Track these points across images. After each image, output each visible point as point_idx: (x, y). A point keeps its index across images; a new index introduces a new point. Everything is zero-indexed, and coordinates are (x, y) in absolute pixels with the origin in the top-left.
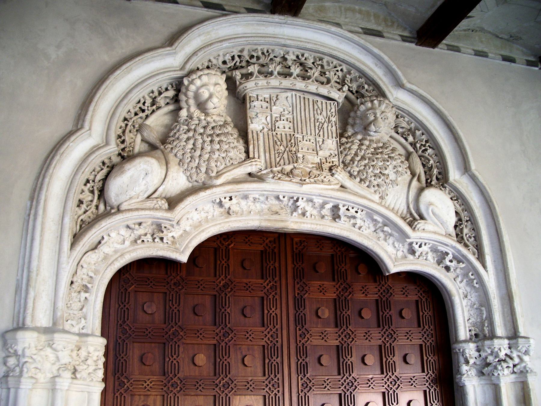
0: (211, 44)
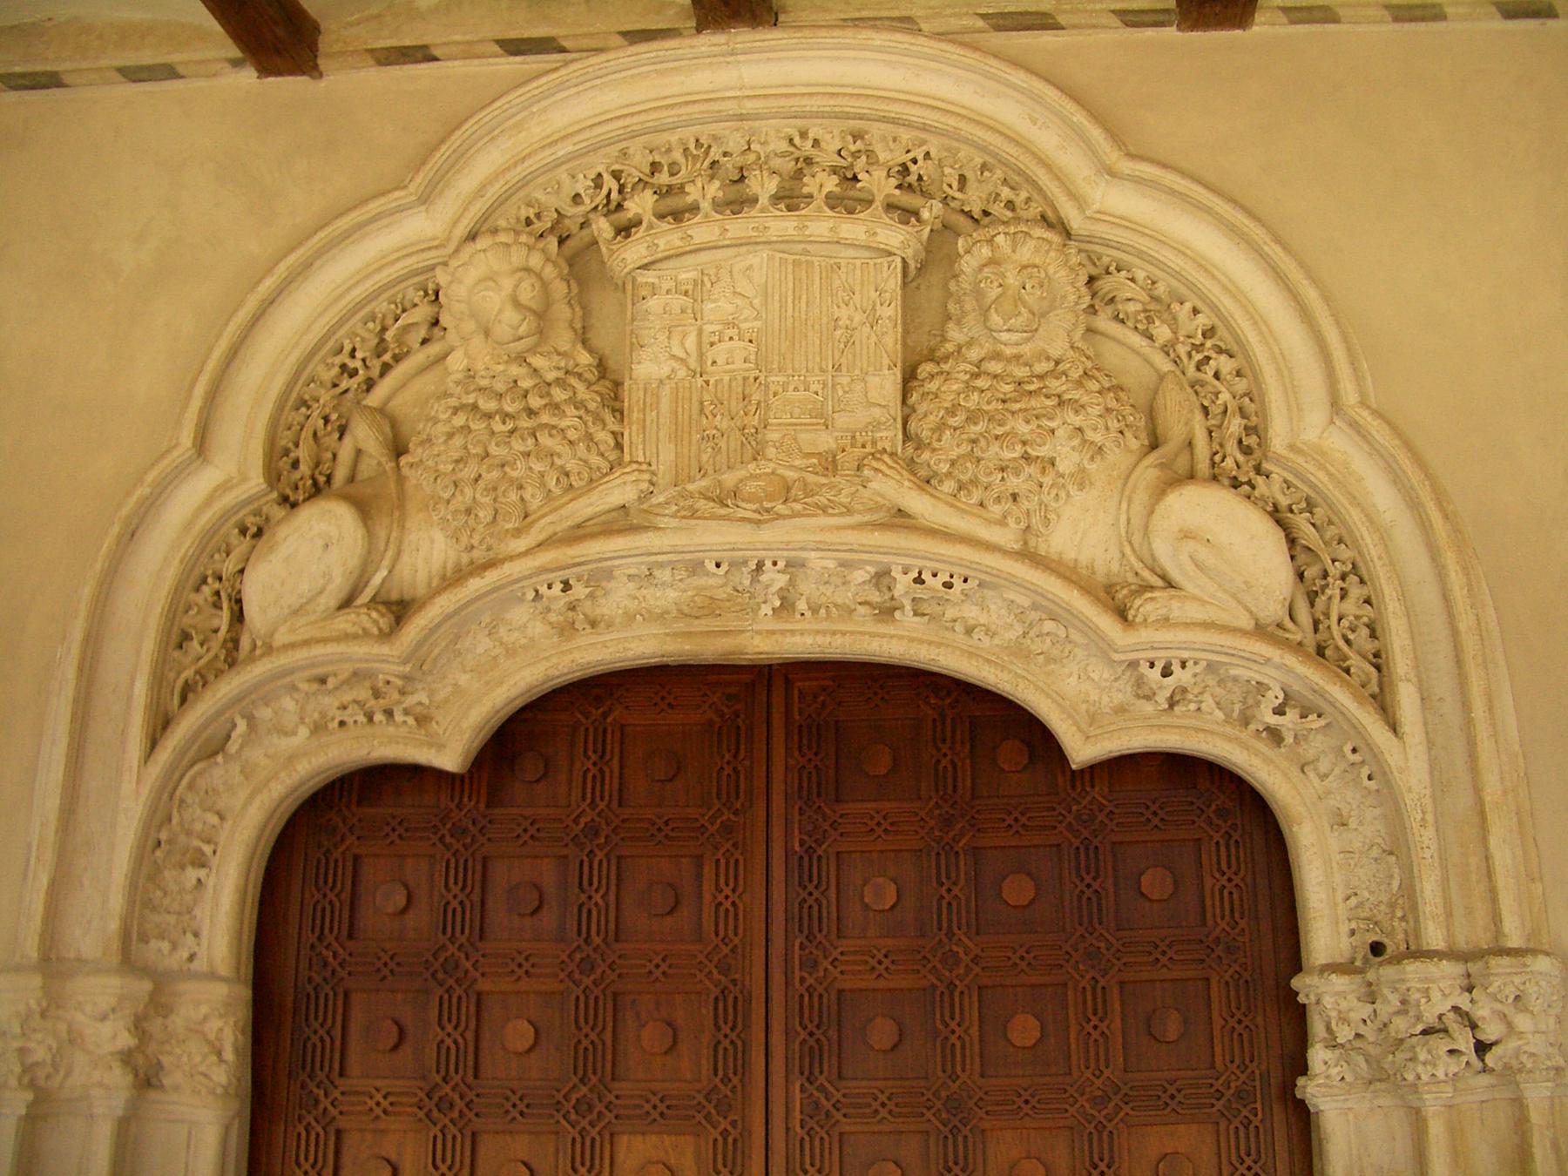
0: (523, 159)
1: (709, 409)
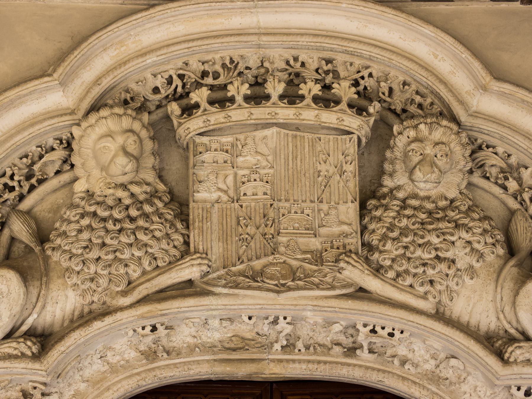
0: (125, 63)
1: (242, 222)
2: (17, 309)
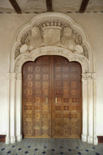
2: (27, 48)
